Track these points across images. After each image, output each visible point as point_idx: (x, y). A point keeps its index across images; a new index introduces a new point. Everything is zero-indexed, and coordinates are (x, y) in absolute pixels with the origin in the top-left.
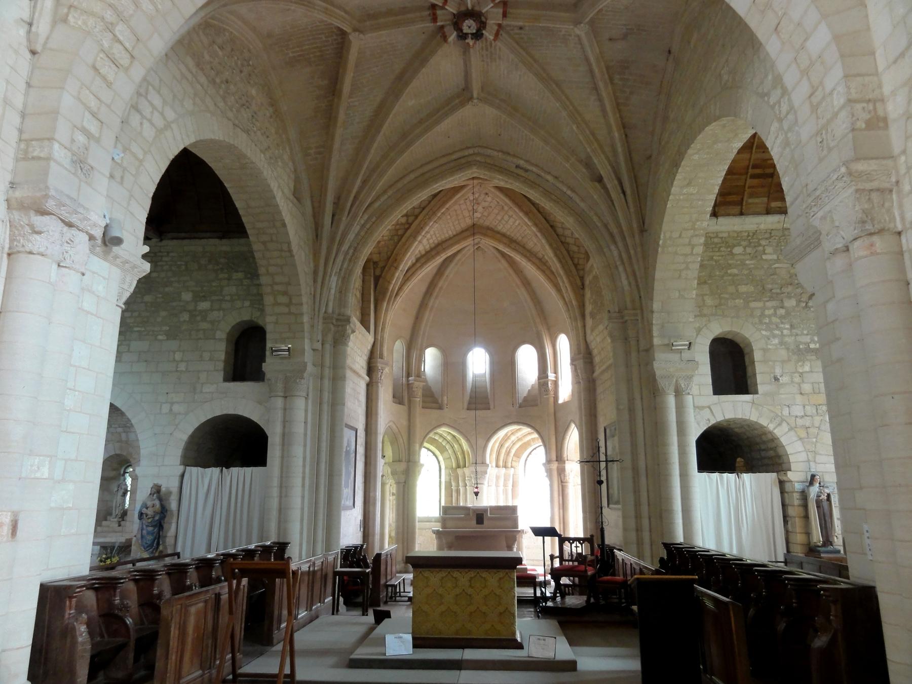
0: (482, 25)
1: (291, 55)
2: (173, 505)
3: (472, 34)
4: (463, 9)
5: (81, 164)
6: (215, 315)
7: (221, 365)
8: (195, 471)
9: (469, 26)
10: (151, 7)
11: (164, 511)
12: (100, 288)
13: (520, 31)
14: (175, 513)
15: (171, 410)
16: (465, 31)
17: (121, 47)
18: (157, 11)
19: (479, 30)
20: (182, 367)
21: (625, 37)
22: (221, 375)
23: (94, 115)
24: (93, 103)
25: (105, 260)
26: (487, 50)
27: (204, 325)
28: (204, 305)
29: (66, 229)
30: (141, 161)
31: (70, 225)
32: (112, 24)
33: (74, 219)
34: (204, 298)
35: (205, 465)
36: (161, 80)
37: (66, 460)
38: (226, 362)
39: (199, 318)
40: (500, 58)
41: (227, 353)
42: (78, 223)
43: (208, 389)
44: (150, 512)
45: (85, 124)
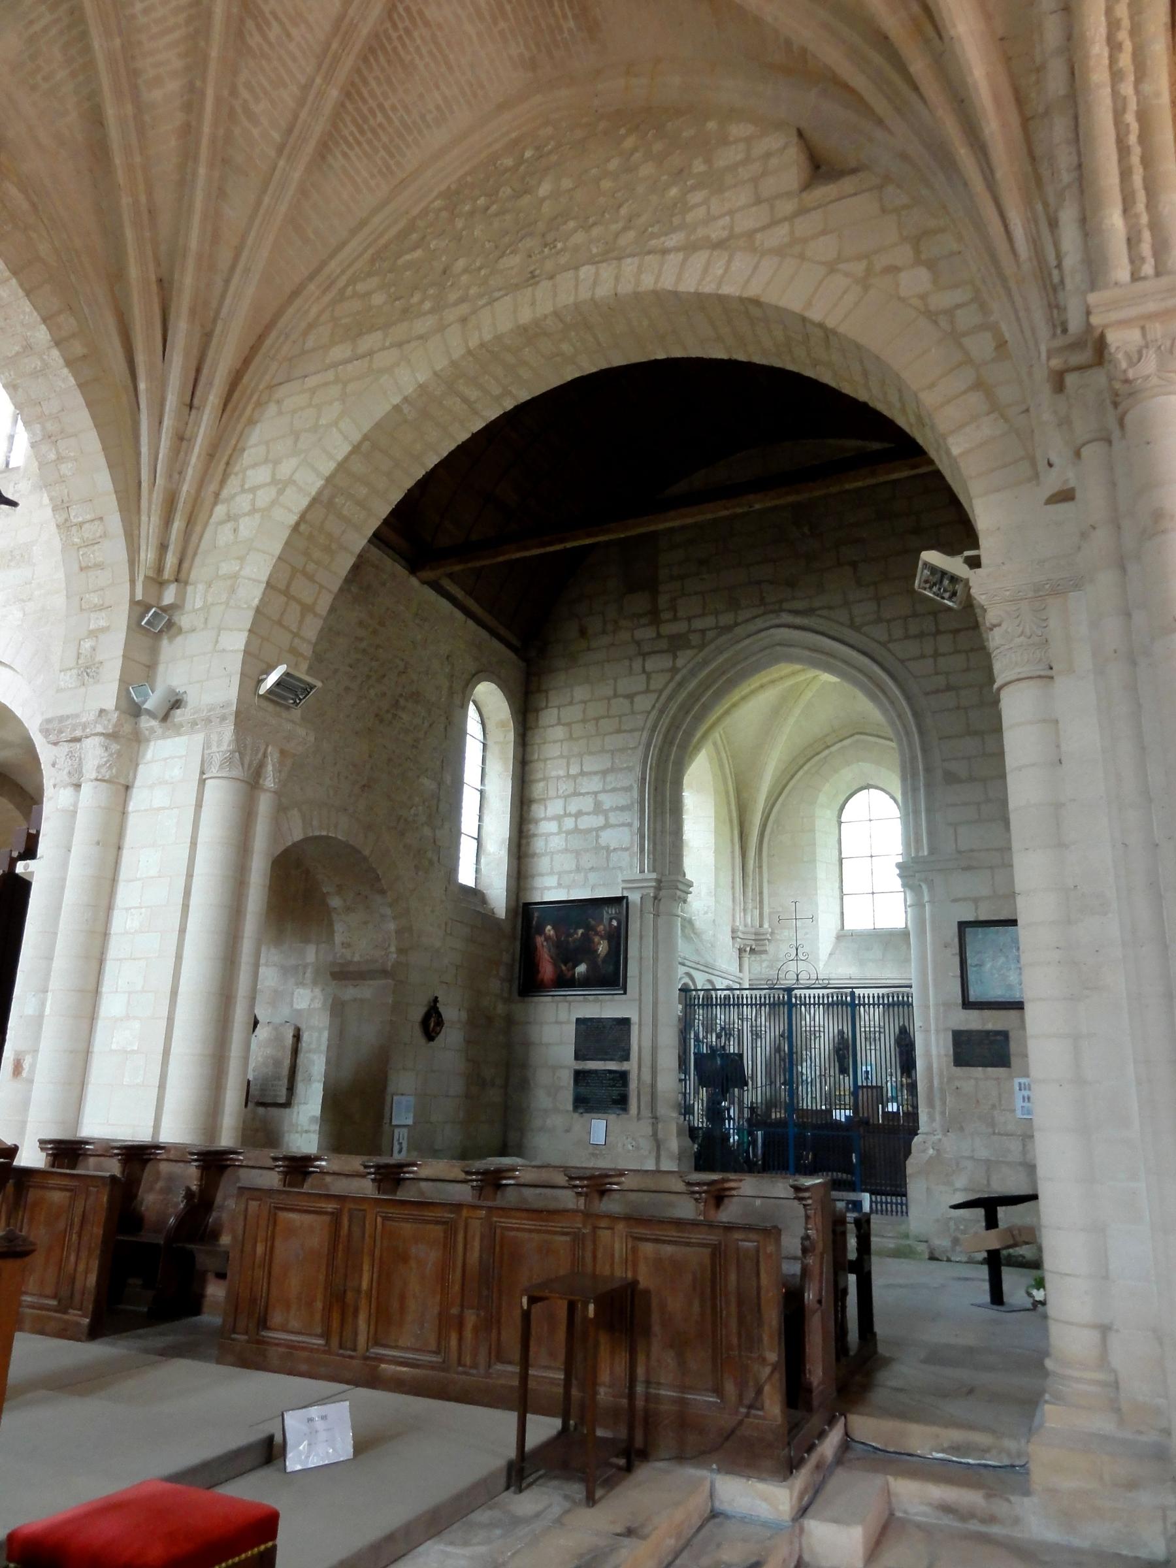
1: (572, 24)
5: (88, 671)
10: (70, 465)
12: (177, 772)
17: (87, 526)
18: (76, 460)
23: (101, 608)
24: (95, 599)
25: (180, 735)
29: (78, 745)
30: (235, 576)
31: (77, 740)
32: (66, 520)
36: (267, 443)
37: (130, 993)
42: (78, 733)
45: (92, 627)
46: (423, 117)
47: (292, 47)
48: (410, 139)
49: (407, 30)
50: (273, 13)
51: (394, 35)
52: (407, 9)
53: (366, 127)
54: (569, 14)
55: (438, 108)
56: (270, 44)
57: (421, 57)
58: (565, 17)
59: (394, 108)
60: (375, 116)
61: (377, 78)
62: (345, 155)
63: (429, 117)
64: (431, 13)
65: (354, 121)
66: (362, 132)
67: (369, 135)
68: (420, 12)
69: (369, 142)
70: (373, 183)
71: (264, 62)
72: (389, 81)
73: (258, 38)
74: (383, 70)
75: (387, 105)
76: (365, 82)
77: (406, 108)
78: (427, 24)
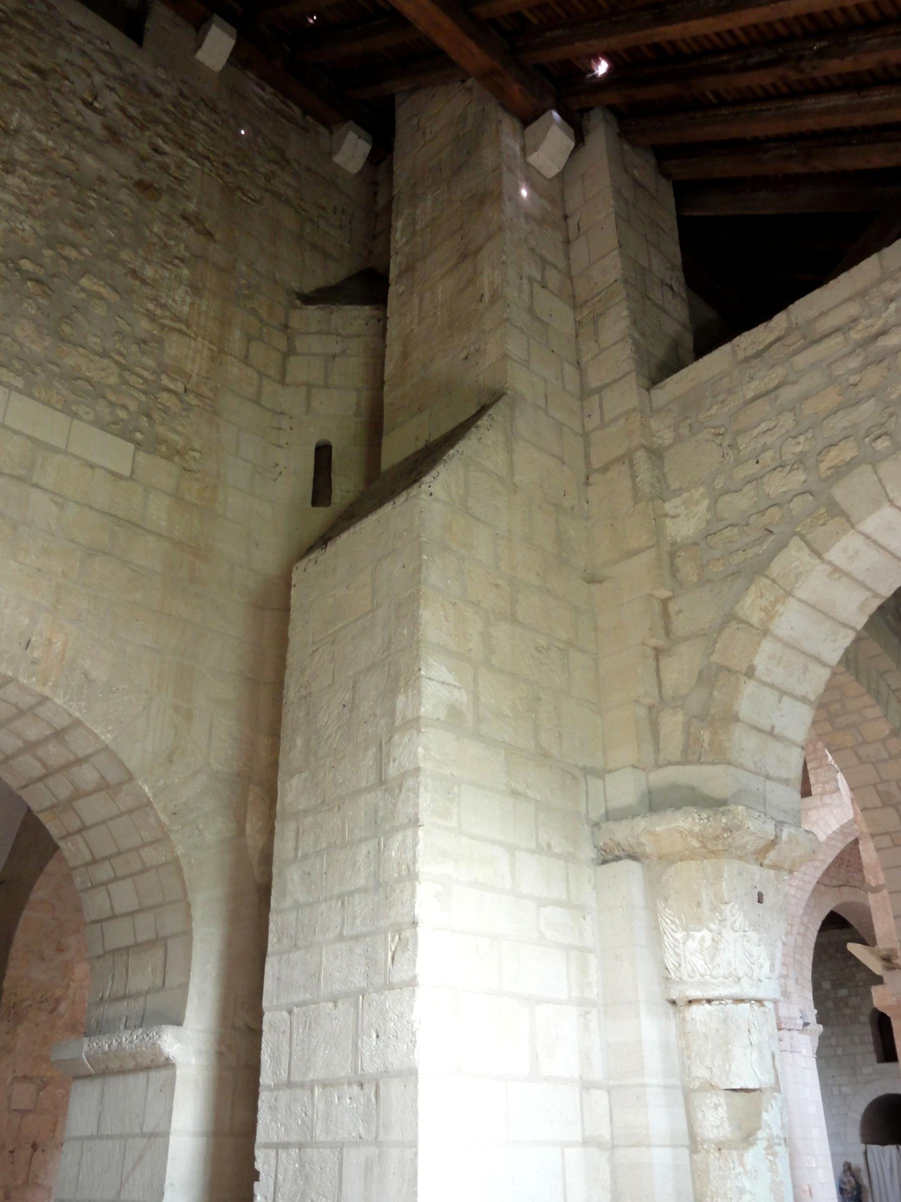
2: (865, 1181)
6: (854, 1001)
7: (871, 1048)
8: (875, 1149)
11: (859, 1187)
14: (869, 1189)
15: (840, 1092)
20: (840, 1051)
22: (873, 1058)
27: (847, 1011)
28: (843, 992)
33: (792, 1027)
34: (842, 986)
35: (883, 1143)
38: (875, 1043)
39: (841, 1004)
41: (873, 1035)
43: (866, 1070)
44: (847, 1187)
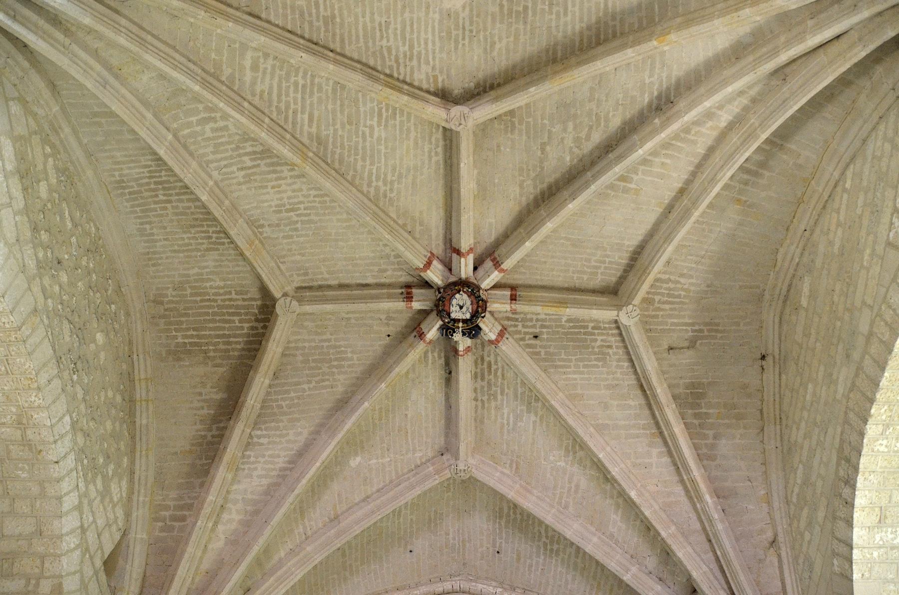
0: (480, 307)
1: (180, 340)
3: (465, 321)
4: (453, 279)
9: (460, 307)
13: (534, 342)
16: (453, 316)
19: (475, 315)
21: (692, 344)
26: (483, 379)
40: (502, 393)
46: (150, 223)
47: (234, 168)
48: (138, 209)
49: (210, 237)
50: (259, 165)
51: (211, 230)
52: (223, 244)
53: (160, 187)
54: (186, 341)
55: (153, 234)
56: (240, 156)
57: (189, 238)
58: (186, 337)
59: (165, 208)
60: (164, 195)
61: (189, 208)
62: (146, 166)
63: (148, 227)
64: (214, 255)
65: (168, 182)
66: (156, 183)
67: (152, 186)
68: (218, 250)
69: (148, 184)
70: (117, 173)
71: (233, 146)
72: (182, 214)
73: (249, 149)
74: (192, 213)
75: (168, 205)
76: (189, 200)
77: (162, 216)
78: (208, 250)
